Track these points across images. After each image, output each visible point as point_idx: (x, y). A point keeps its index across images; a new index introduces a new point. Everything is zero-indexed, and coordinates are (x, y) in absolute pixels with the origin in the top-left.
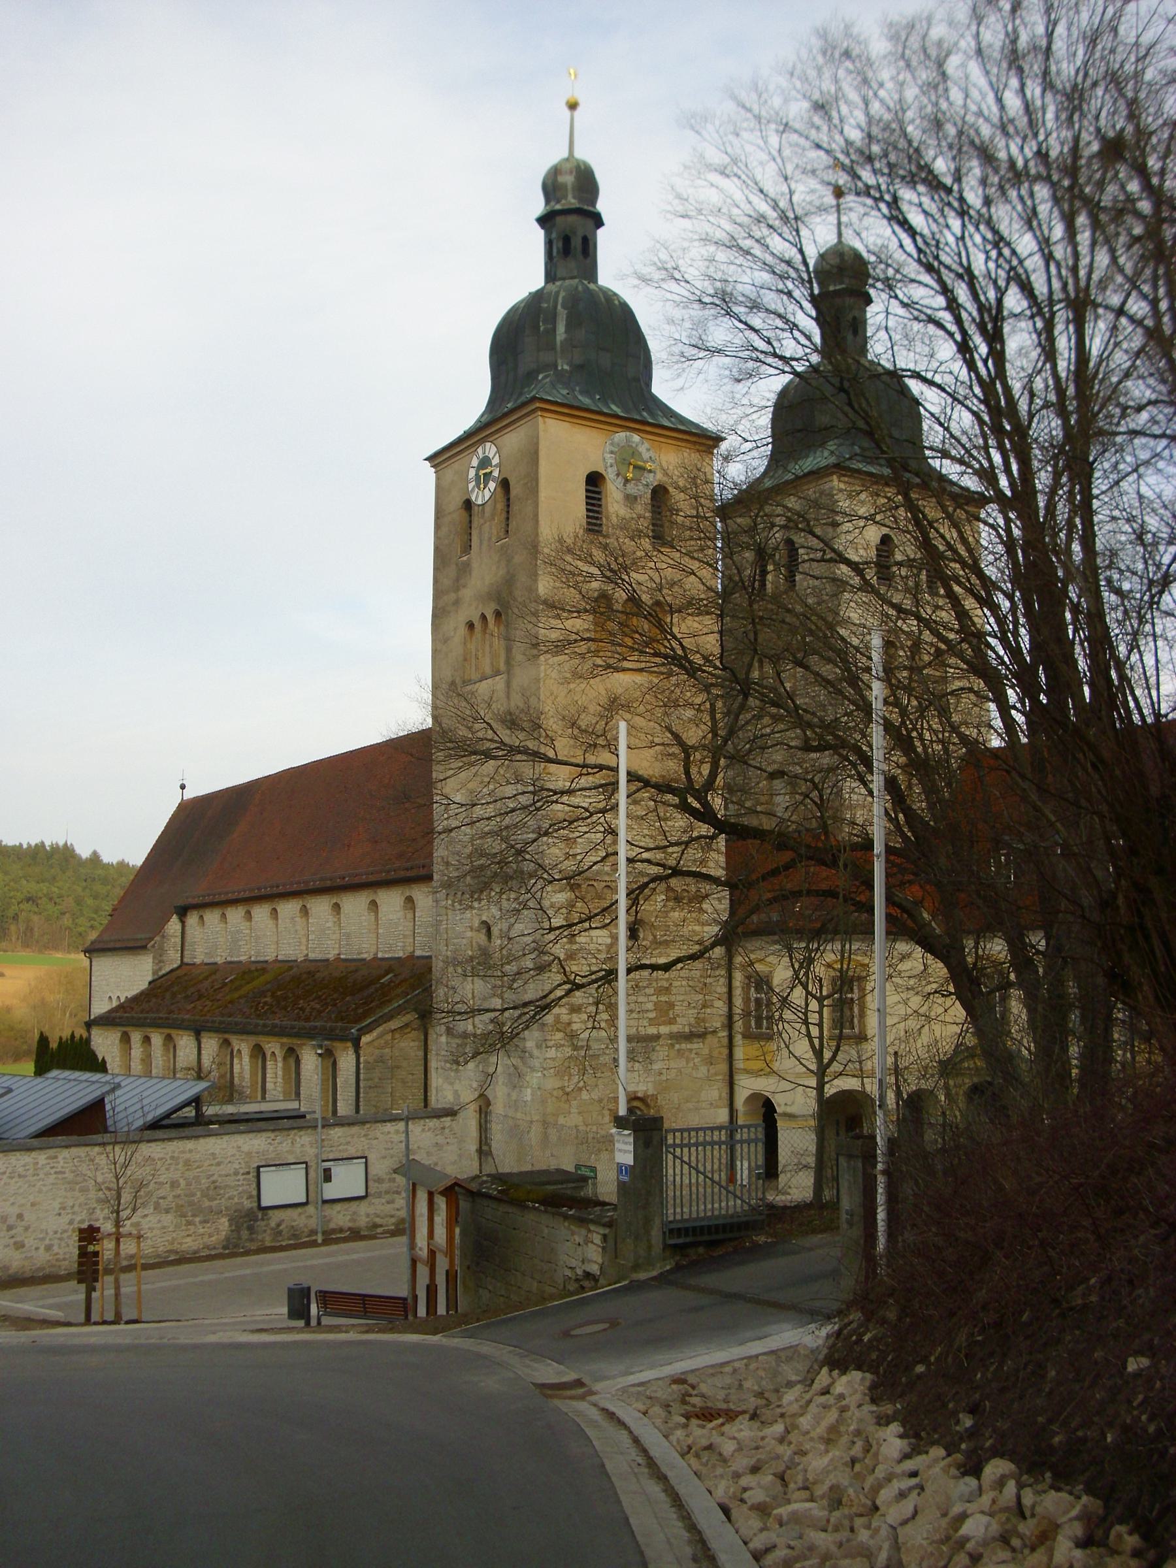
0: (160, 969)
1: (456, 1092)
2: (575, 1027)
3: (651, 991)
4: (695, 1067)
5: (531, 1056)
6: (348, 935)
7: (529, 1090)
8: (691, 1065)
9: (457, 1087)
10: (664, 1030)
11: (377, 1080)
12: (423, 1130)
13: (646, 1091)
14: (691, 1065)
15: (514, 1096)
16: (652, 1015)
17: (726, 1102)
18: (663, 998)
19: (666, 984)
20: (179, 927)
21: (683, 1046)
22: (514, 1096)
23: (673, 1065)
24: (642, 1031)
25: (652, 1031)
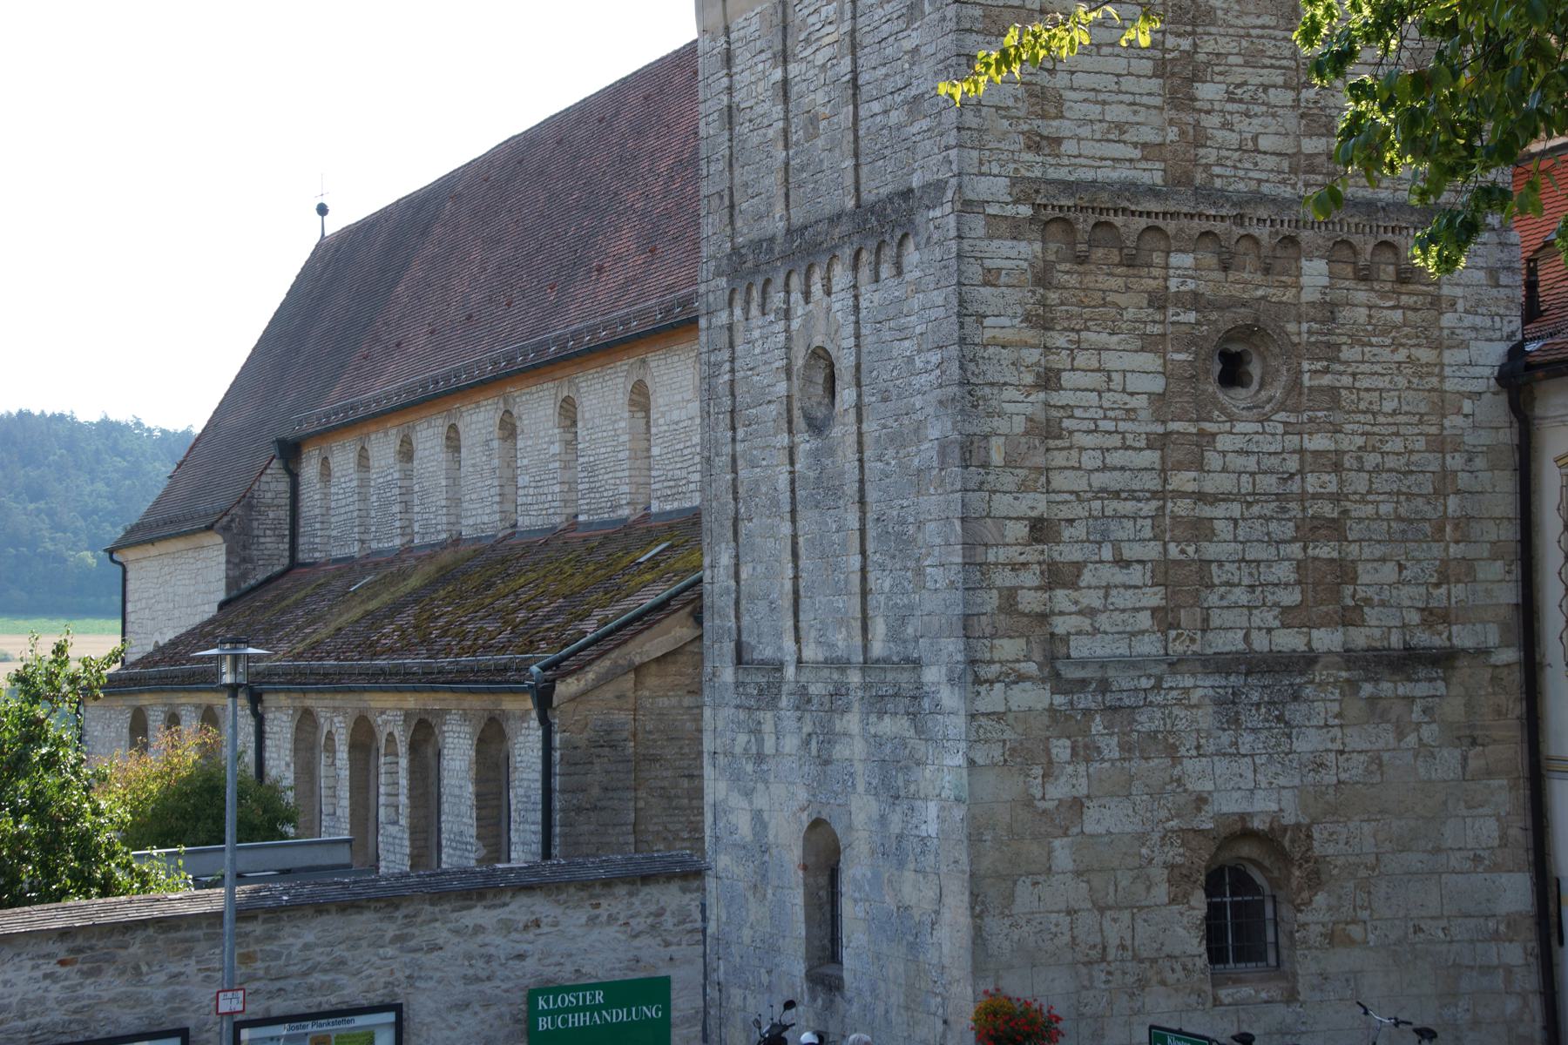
0: (244, 576)
1: (757, 816)
2: (1061, 625)
3: (1289, 530)
4: (1425, 751)
5: (937, 708)
6: (591, 469)
7: (932, 809)
8: (1411, 739)
9: (760, 801)
10: (1327, 639)
11: (596, 791)
12: (592, 920)
13: (1276, 816)
15: (896, 823)
16: (1292, 597)
17: (1525, 857)
18: (1326, 551)
19: (1329, 510)
20: (284, 486)
21: (1386, 687)
22: (896, 823)
23: (1356, 740)
24: (1260, 643)
25: (1290, 641)
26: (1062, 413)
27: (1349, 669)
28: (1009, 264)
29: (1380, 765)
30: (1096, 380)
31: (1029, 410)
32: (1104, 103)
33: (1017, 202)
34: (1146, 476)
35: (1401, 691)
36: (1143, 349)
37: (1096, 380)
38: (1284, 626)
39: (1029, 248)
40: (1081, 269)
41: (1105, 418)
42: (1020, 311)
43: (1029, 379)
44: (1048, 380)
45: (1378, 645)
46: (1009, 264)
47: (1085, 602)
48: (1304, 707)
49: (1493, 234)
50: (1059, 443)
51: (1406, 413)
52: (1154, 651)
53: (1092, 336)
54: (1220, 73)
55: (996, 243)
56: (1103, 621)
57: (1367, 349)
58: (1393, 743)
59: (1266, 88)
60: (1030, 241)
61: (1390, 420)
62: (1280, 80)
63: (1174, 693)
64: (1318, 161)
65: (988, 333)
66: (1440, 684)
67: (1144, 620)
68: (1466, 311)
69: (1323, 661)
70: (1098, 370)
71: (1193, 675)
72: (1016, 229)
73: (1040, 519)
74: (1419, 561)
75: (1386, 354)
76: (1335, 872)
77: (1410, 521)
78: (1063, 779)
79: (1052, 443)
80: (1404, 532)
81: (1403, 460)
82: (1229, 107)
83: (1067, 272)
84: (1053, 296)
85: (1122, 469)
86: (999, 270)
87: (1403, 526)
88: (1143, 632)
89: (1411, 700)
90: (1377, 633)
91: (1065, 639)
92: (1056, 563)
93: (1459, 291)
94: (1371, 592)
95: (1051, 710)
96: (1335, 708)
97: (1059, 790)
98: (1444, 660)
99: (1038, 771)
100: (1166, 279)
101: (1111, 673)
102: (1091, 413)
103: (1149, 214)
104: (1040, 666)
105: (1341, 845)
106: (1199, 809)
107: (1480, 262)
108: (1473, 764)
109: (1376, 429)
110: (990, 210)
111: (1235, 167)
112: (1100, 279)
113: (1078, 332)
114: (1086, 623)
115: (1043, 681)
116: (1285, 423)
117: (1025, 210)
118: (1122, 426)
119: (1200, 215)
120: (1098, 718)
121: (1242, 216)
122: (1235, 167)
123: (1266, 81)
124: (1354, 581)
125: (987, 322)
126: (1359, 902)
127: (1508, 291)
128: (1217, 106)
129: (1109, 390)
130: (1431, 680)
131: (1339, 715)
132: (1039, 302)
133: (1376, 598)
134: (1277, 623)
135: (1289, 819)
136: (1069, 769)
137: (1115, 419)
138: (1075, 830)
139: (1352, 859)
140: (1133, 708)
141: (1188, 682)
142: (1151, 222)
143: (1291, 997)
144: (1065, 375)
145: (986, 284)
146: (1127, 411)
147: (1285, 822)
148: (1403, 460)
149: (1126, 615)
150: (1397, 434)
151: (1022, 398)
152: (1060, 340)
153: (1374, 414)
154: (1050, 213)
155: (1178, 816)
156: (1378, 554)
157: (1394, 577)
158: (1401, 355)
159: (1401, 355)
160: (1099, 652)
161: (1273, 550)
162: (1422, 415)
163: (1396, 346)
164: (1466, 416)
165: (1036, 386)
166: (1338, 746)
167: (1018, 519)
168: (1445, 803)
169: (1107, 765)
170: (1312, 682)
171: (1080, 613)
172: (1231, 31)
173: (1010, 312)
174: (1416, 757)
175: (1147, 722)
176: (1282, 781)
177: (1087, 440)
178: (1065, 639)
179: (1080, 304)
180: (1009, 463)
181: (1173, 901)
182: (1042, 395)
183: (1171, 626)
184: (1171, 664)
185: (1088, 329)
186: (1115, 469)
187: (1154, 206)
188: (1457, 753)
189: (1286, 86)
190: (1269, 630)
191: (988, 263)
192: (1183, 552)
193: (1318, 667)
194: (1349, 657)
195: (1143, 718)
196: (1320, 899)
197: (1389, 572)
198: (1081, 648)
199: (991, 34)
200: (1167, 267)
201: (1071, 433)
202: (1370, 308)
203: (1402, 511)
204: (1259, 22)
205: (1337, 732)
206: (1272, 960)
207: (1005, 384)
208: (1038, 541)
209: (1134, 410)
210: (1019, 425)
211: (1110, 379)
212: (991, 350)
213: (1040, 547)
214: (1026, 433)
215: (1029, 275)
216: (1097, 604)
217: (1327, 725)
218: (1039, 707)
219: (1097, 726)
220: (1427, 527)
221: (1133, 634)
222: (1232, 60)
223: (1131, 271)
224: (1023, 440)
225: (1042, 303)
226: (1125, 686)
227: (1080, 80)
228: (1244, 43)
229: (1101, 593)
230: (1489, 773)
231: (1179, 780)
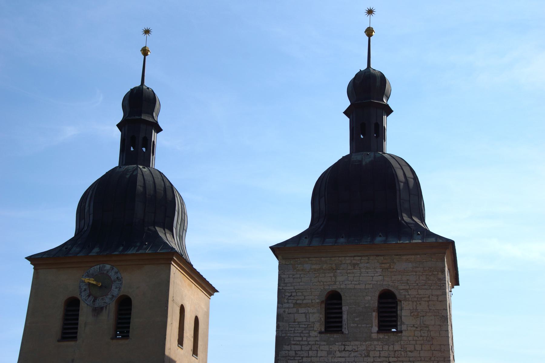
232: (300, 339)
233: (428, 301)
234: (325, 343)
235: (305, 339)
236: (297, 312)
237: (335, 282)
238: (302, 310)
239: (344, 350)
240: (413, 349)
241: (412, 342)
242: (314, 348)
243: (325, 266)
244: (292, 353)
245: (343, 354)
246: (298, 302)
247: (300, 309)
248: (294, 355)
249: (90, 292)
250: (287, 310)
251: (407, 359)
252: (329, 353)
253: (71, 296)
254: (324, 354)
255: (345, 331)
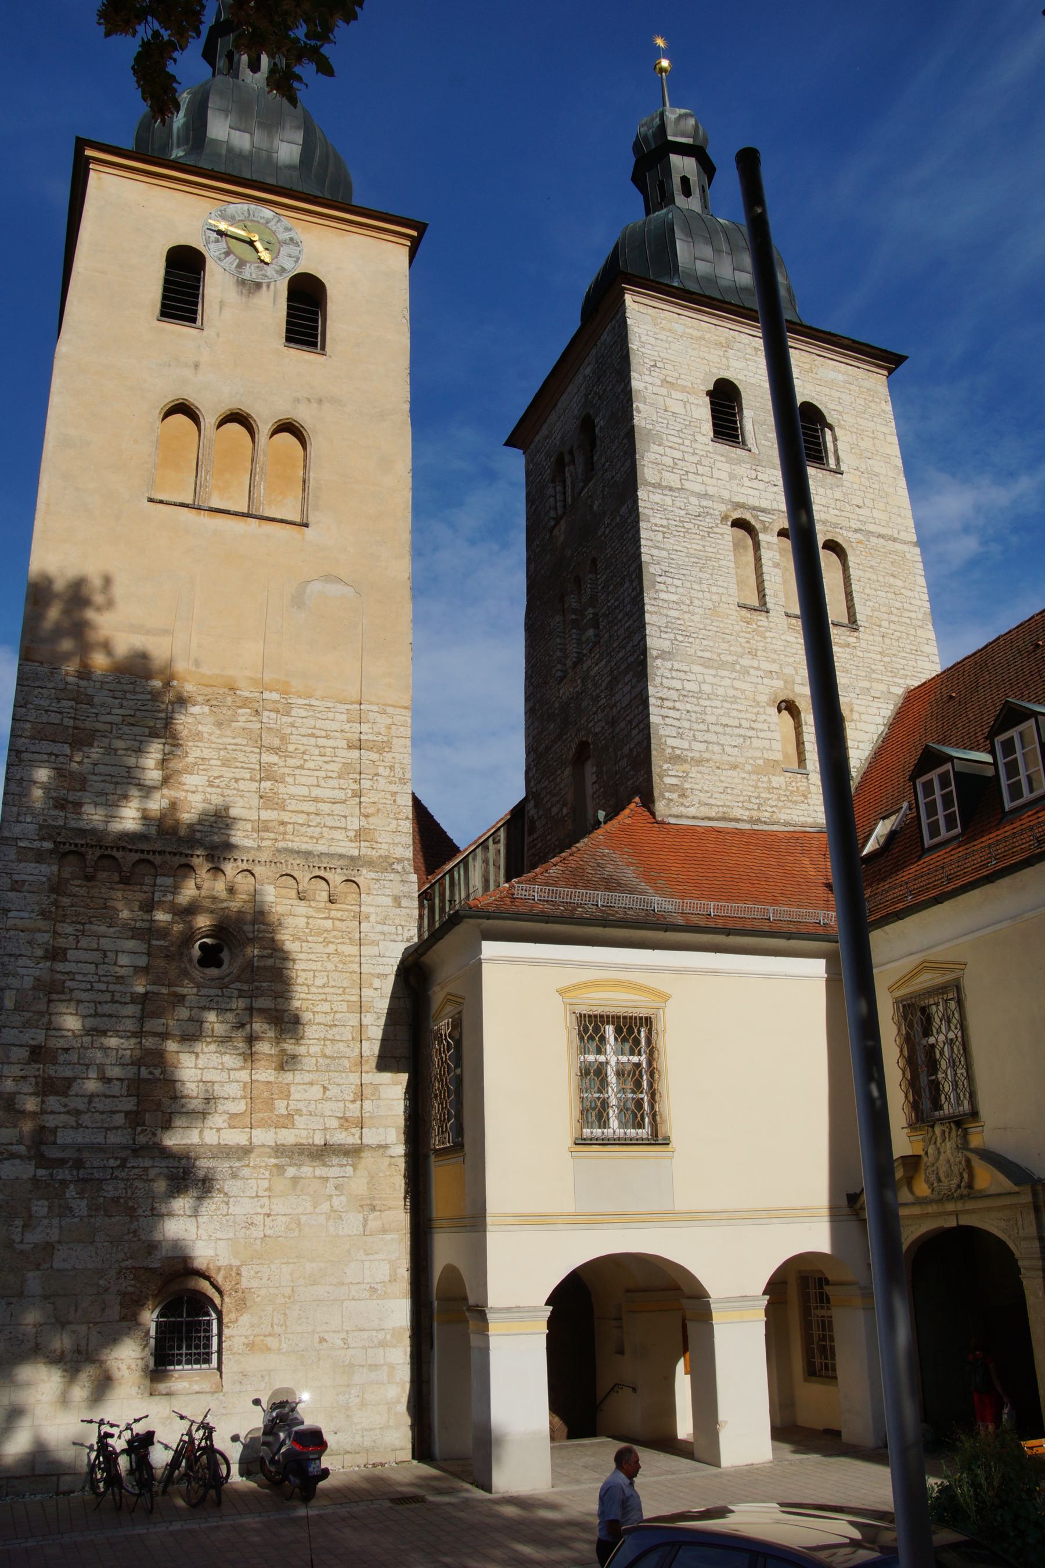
8: (325, 1207)
10: (263, 1137)
14: (325, 1207)
23: (279, 1206)
26: (66, 977)
27: (277, 1157)
28: (31, 878)
29: (299, 1224)
30: (97, 956)
31: (38, 973)
32: (117, 783)
33: (42, 839)
34: (128, 1022)
35: (318, 1173)
36: (132, 938)
37: (97, 956)
38: (230, 1127)
39: (48, 870)
40: (89, 884)
41: (99, 981)
42: (36, 908)
43: (40, 953)
44: (55, 954)
45: (305, 1142)
46: (31, 878)
47: (72, 1105)
48: (240, 1183)
49: (398, 875)
50: (62, 997)
51: (333, 987)
52: (124, 1141)
53: (94, 928)
54: (204, 770)
55: (22, 865)
56: (86, 1119)
57: (304, 944)
58: (310, 1209)
59: (237, 780)
60: (50, 864)
61: (320, 990)
62: (248, 776)
63: (136, 1171)
64: (271, 824)
65: (10, 922)
66: (350, 1169)
67: (119, 1120)
68: (378, 923)
69: (256, 1151)
70: (97, 950)
71: (153, 1158)
72: (40, 857)
73: (40, 1047)
74: (338, 1085)
75: (320, 948)
76: (258, 1300)
77: (333, 1058)
78: (40, 1229)
79: (54, 996)
80: (328, 1065)
81: (329, 1018)
82: (209, 790)
83: (78, 886)
84: (66, 901)
85: (110, 1016)
86: (24, 881)
87: (328, 1061)
88: (117, 1128)
89: (327, 1179)
90: (304, 1133)
91: (54, 1131)
92: (50, 1077)
93: (372, 910)
94: (300, 1105)
95: (34, 1179)
96: (265, 1184)
97: (34, 1237)
98: (353, 1152)
99: (19, 1222)
100: (153, 894)
101: (85, 1155)
102: (89, 978)
103: (142, 851)
104: (29, 1148)
105: (265, 1281)
106: (150, 1254)
107: (388, 892)
108: (372, 1224)
109: (309, 996)
110: (21, 844)
111: (211, 826)
112: (103, 891)
113: (83, 924)
114: (72, 1120)
115: (30, 1158)
116: (240, 990)
117: (48, 845)
118: (112, 987)
119: (181, 854)
120: (72, 1187)
121: (213, 856)
122: (211, 826)
123: (238, 777)
124: (288, 1097)
125: (10, 915)
126: (276, 1321)
127: (408, 911)
128: (200, 789)
129: (104, 963)
130: (342, 1166)
131: (269, 1189)
132: (53, 904)
133: (304, 1110)
134: (226, 1125)
135: (223, 1262)
136: (45, 1222)
137: (107, 983)
138: (46, 1266)
139: (271, 1290)
140: (100, 1180)
141: (148, 1163)
142: (143, 856)
143: (219, 1388)
144: (70, 952)
145: (12, 890)
146: (118, 977)
147: (219, 1264)
148: (329, 1018)
149: (105, 1116)
150: (326, 1000)
151: (32, 965)
152: (69, 929)
153: (308, 986)
154: (67, 848)
155: (131, 1258)
156: (307, 1080)
157: (320, 1095)
158: (331, 949)
159: (331, 949)
160: (80, 1140)
161: (225, 1075)
162: (345, 988)
163: (327, 942)
164: (376, 989)
165: (45, 958)
166: (266, 1210)
167: (21, 1046)
168: (349, 1251)
169: (77, 1220)
170: (248, 1166)
171: (68, 1113)
172: (213, 746)
173: (29, 908)
174: (328, 1219)
175: (110, 1190)
176: (219, 1235)
177: (85, 996)
178: (54, 1131)
179: (87, 906)
180: (18, 1008)
181: (123, 1319)
182: (48, 964)
183: (138, 1124)
184: (135, 1151)
185: (91, 923)
186: (104, 1015)
187: (145, 847)
188: (360, 1216)
189: (252, 779)
190: (219, 1130)
191: (16, 877)
192: (151, 1073)
193: (253, 1155)
194: (279, 1150)
195: (110, 1188)
196: (245, 1319)
197: (316, 1092)
198: (64, 1137)
199: (35, 738)
200: (155, 885)
201: (71, 991)
202: (308, 918)
203: (328, 1052)
204: (234, 741)
205: (266, 1200)
206: (215, 1363)
207: (20, 955)
208: (36, 1062)
209: (122, 977)
210: (28, 983)
211: (105, 956)
212: (12, 932)
213: (37, 1066)
214: (34, 988)
215: (46, 886)
216: (82, 1107)
217: (257, 1196)
218: (25, 1177)
219: (71, 1191)
220: (346, 1063)
221: (108, 1129)
222: (212, 762)
223: (128, 887)
224: (31, 993)
225: (56, 903)
226: (96, 1164)
227: (101, 769)
228: (222, 753)
229: (86, 1100)
230: (384, 1231)
231: (135, 1232)
232: (680, 441)
233: (874, 438)
234: (722, 459)
235: (687, 443)
236: (669, 396)
237: (728, 367)
238: (676, 395)
239: (756, 478)
240: (861, 504)
241: (858, 493)
242: (705, 461)
243: (707, 336)
244: (670, 462)
245: (755, 484)
246: (668, 379)
247: (673, 392)
248: (672, 464)
249: (229, 248)
250: (650, 387)
251: (856, 517)
252: (732, 476)
253: (183, 242)
254: (725, 476)
255: (754, 450)
